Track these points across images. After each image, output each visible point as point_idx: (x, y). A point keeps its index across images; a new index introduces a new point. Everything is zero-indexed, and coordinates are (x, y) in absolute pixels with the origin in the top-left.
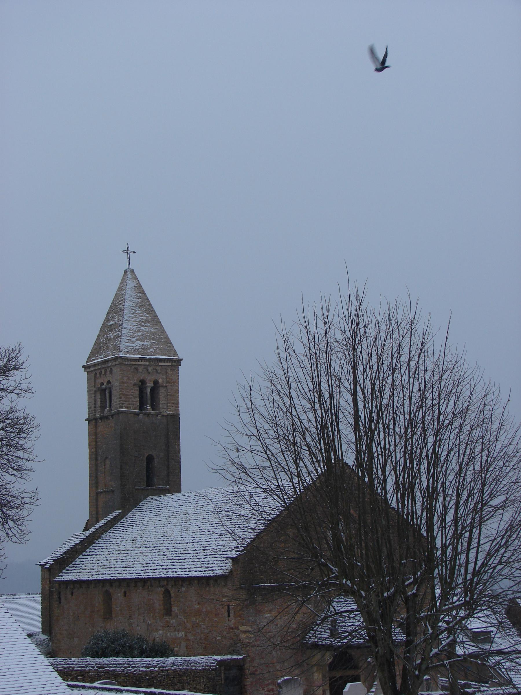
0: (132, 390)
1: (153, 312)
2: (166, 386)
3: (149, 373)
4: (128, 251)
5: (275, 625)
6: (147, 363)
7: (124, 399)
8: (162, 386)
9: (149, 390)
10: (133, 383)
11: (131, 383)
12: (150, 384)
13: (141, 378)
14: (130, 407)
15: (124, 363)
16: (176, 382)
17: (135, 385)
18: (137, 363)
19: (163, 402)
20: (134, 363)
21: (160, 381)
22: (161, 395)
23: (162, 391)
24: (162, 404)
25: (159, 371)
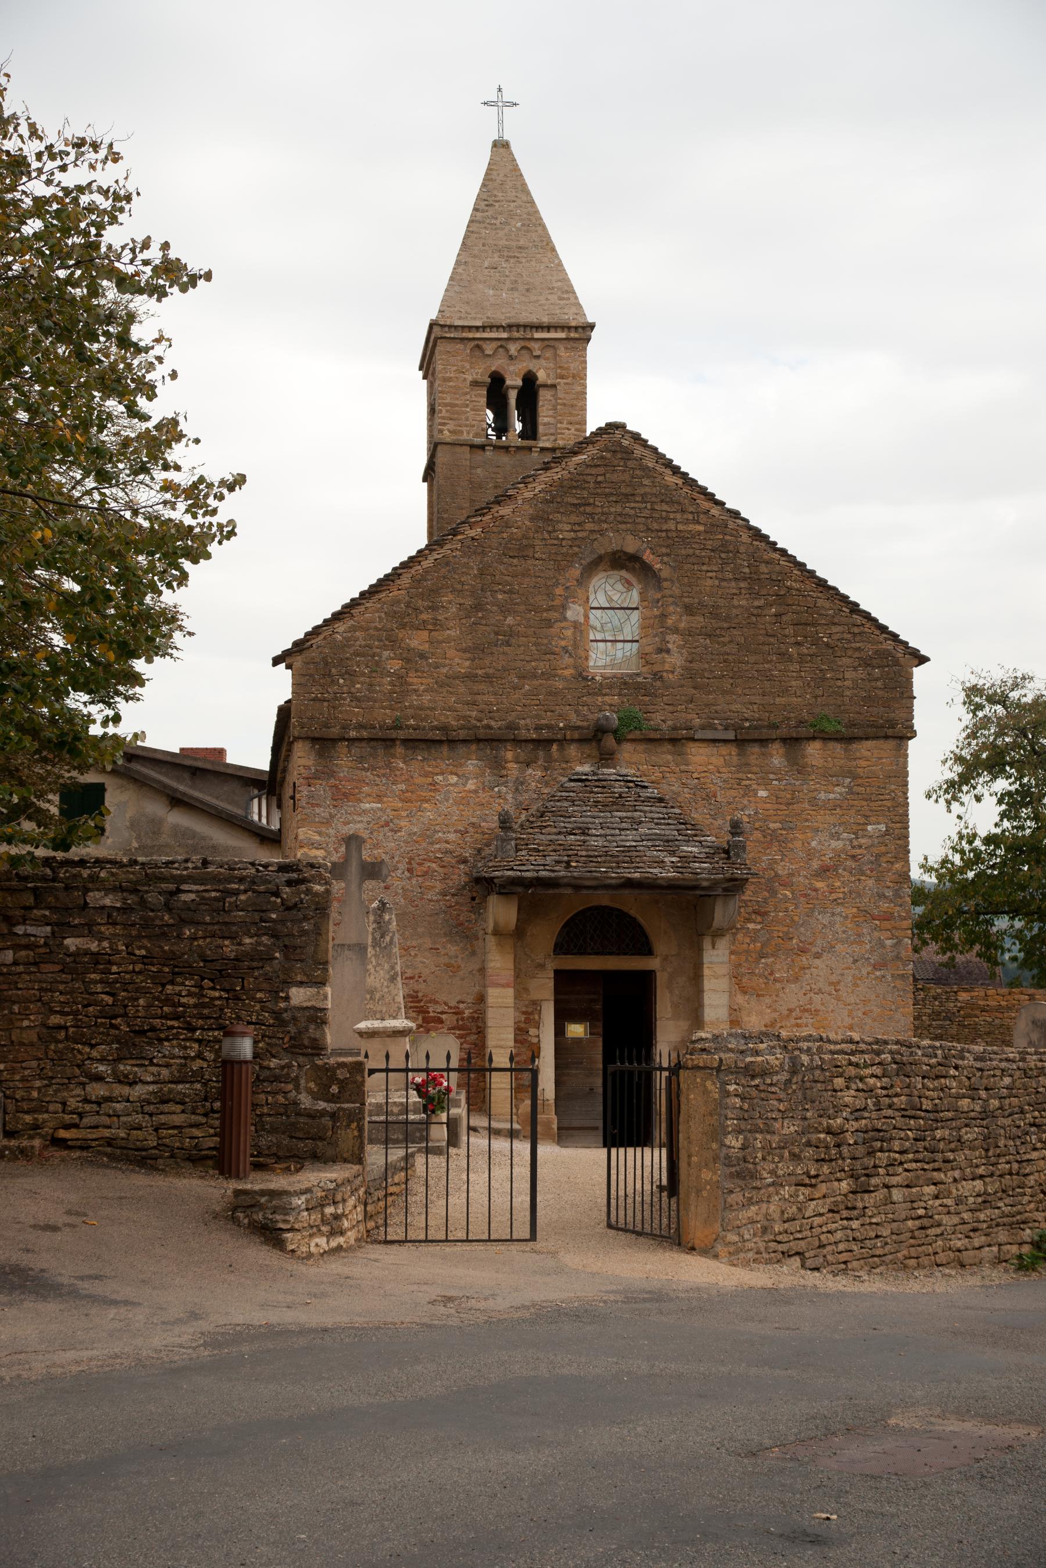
0: (466, 394)
1: (539, 229)
2: (554, 386)
3: (511, 358)
4: (500, 103)
5: (392, 830)
6: (505, 335)
7: (447, 415)
8: (545, 386)
9: (513, 396)
10: (470, 378)
11: (465, 379)
12: (514, 381)
13: (493, 369)
14: (462, 432)
15: (448, 335)
16: (580, 376)
17: (475, 384)
18: (478, 335)
19: (546, 420)
20: (471, 335)
21: (542, 376)
22: (543, 406)
23: (544, 397)
24: (545, 424)
25: (537, 353)
